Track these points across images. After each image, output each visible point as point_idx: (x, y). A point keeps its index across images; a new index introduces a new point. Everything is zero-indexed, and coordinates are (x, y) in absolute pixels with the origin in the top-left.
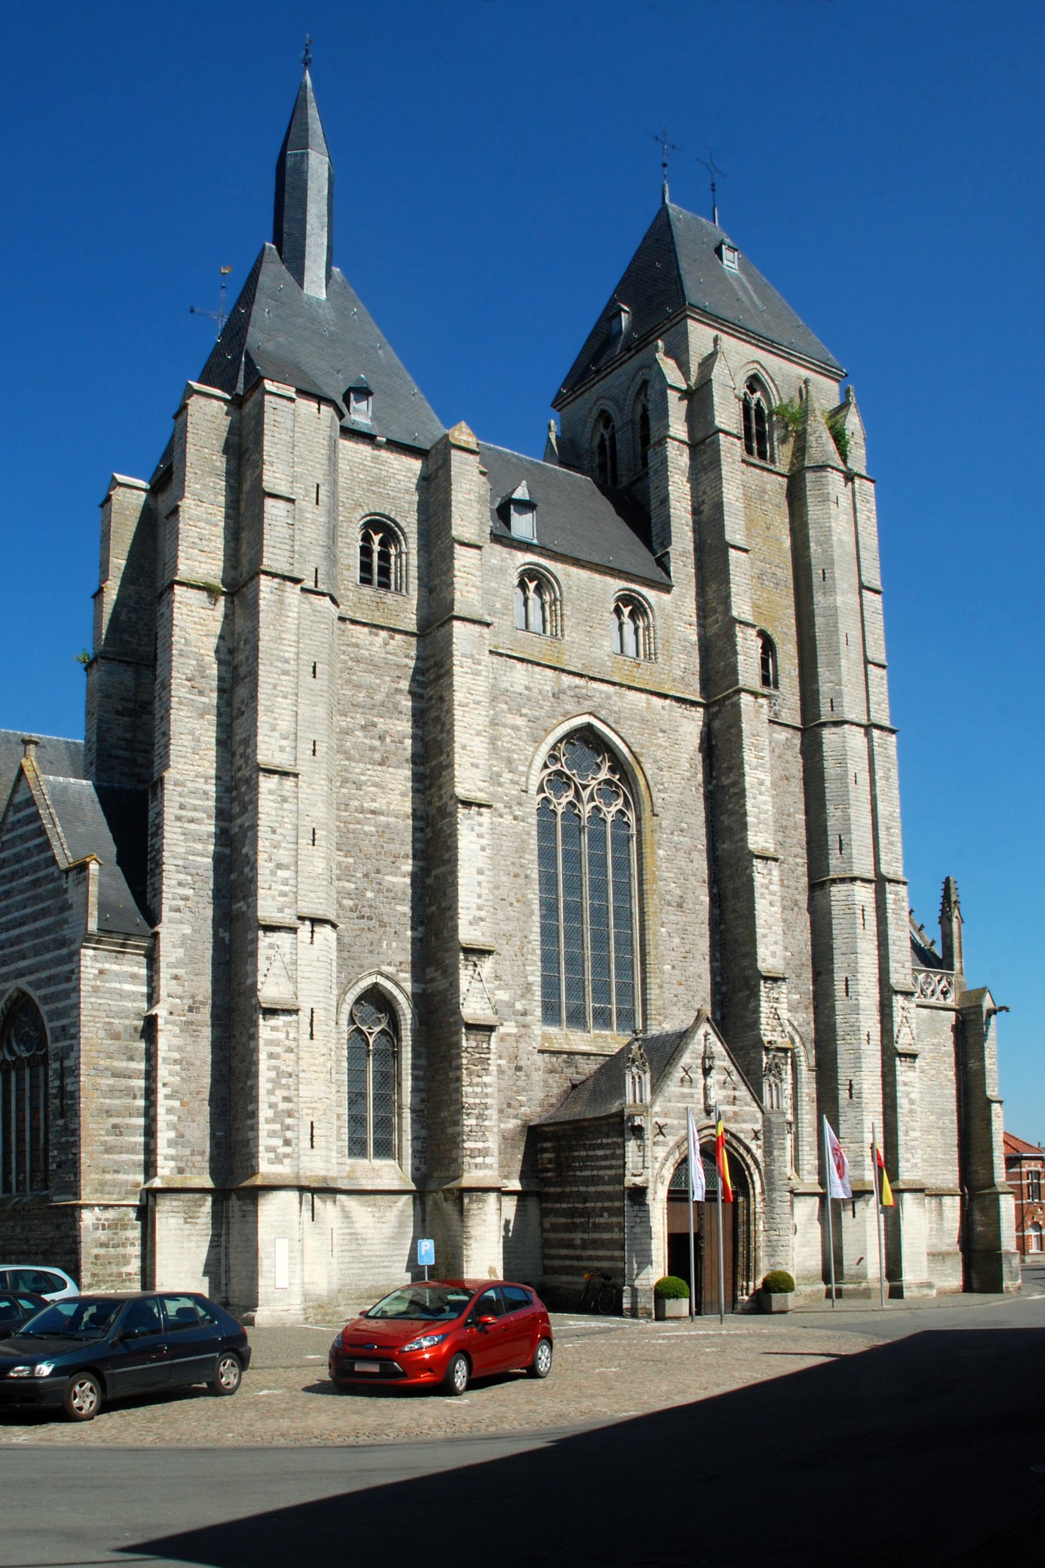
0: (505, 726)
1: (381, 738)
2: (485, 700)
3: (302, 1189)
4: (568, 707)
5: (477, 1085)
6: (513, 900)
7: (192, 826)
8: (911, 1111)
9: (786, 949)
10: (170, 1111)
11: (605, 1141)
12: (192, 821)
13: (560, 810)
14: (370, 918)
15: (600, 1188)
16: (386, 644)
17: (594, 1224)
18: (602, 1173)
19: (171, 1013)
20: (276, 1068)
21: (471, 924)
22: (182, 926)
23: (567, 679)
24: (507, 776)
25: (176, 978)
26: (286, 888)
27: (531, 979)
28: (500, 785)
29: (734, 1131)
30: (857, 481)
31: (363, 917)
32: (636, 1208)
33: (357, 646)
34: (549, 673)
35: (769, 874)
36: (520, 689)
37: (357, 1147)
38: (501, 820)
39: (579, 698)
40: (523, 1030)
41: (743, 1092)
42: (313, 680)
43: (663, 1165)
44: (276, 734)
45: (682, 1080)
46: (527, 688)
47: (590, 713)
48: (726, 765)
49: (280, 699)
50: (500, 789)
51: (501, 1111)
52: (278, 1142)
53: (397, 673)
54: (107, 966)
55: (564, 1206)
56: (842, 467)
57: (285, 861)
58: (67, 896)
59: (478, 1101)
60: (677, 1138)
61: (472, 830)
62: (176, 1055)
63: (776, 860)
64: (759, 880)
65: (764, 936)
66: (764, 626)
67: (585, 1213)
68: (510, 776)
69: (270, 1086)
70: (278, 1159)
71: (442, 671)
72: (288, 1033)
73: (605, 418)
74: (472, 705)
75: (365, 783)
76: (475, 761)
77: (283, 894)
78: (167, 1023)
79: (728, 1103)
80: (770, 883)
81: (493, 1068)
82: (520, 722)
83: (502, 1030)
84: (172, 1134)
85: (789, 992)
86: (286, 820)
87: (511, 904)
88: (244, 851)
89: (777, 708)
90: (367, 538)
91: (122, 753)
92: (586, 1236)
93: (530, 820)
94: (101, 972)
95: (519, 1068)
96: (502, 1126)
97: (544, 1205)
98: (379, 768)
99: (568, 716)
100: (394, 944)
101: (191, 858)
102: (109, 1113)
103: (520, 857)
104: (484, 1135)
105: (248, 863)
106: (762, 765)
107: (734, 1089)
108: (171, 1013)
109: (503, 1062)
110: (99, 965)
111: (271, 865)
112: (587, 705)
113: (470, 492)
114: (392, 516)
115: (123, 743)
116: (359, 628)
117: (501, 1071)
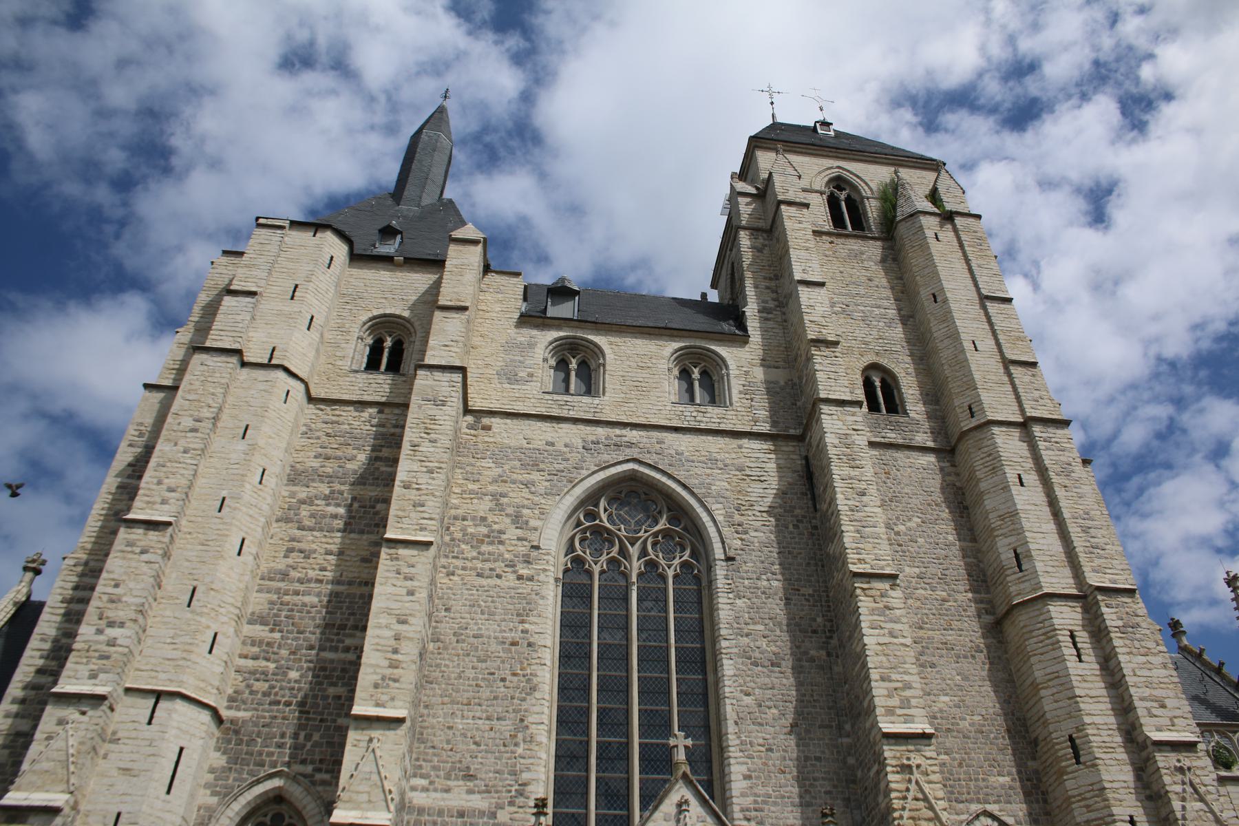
6: (507, 674)
28: (501, 543)
30: (959, 221)
31: (278, 703)
38: (498, 582)
56: (936, 210)
87: (503, 680)
103: (522, 622)
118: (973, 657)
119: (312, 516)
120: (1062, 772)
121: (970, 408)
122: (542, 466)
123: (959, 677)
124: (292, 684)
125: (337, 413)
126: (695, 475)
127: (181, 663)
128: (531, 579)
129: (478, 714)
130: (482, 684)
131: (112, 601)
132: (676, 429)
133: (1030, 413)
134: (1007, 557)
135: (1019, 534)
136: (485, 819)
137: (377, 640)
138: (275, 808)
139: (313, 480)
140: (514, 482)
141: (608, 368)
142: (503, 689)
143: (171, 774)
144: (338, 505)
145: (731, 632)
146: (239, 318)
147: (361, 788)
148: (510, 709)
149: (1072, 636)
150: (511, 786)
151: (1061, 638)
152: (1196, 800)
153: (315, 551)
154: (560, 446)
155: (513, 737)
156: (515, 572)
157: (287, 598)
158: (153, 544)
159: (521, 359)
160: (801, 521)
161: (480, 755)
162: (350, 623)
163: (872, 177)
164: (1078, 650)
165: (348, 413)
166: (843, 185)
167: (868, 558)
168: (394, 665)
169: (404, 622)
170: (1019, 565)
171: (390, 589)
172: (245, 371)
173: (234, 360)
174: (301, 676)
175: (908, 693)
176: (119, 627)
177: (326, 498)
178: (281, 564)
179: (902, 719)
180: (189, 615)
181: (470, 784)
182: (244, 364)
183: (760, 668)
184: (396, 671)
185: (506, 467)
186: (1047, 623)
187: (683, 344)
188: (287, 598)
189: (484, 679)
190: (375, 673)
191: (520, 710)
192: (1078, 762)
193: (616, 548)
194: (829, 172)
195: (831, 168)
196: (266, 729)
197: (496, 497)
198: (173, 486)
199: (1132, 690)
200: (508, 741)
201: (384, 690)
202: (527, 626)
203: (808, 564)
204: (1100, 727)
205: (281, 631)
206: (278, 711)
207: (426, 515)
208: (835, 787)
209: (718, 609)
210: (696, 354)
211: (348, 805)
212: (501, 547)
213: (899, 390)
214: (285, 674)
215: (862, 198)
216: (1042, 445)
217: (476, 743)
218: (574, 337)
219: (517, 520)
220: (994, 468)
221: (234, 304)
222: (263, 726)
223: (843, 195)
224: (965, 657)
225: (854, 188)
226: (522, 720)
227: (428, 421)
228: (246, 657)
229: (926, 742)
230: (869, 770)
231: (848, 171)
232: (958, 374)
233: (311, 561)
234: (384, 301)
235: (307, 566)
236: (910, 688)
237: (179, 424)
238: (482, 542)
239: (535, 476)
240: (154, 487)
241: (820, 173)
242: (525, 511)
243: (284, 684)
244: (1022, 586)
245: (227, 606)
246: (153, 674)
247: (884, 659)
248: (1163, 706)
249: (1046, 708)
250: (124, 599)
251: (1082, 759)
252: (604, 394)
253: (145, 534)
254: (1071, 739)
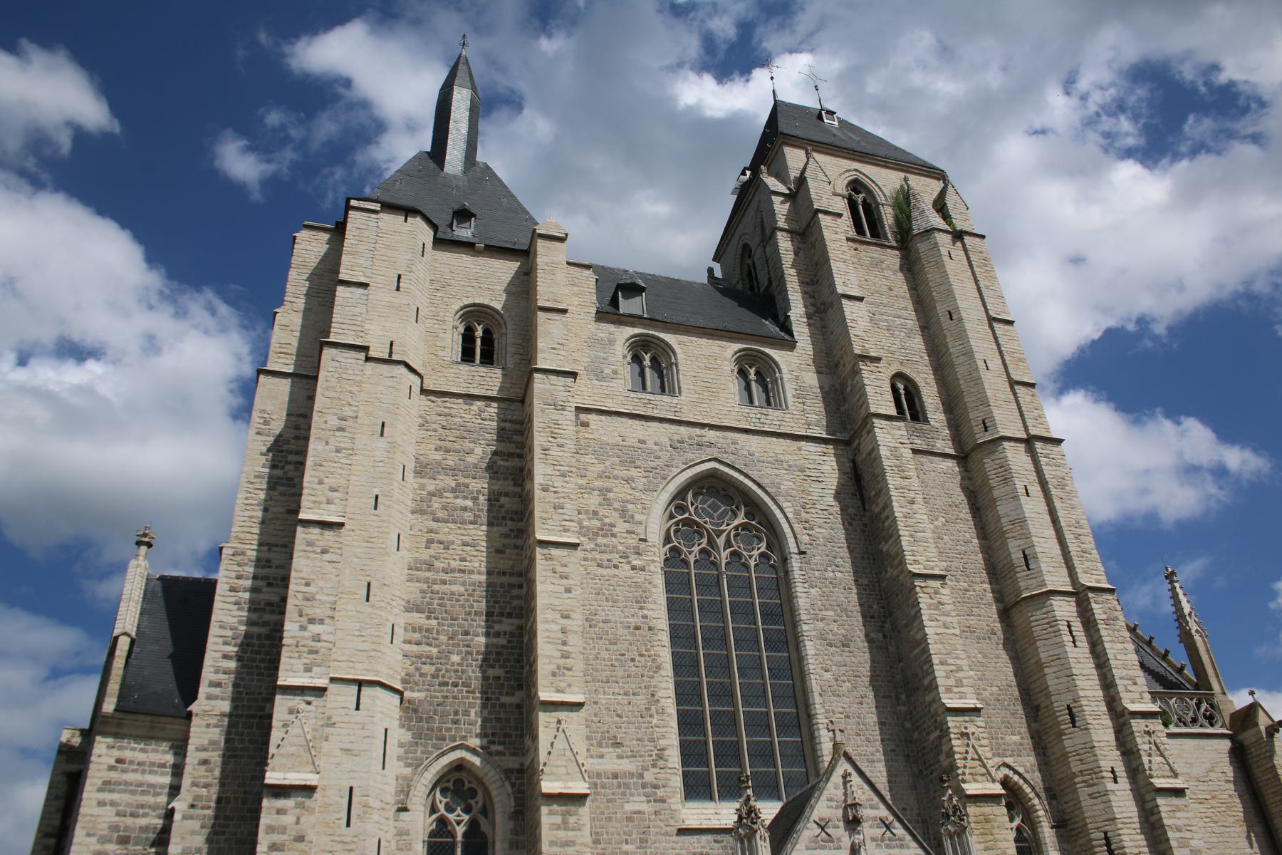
6: (635, 654)
13: (692, 559)
16: (482, 411)
28: (613, 535)
30: (967, 239)
31: (446, 684)
38: (616, 572)
47: (715, 460)
48: (873, 493)
56: (949, 229)
87: (633, 660)
98: (471, 526)
103: (641, 608)
108: (192, 806)
118: (989, 638)
119: (444, 508)
120: (1061, 733)
121: (984, 423)
122: (638, 463)
123: (980, 656)
124: (456, 667)
125: (448, 405)
126: (766, 474)
127: (372, 654)
128: (643, 569)
129: (617, 691)
130: (617, 665)
131: (308, 600)
132: (746, 431)
133: (1033, 431)
134: (1017, 557)
135: (1027, 538)
136: (635, 780)
137: (547, 634)
138: (457, 775)
139: (438, 473)
140: (616, 478)
141: (680, 367)
142: (633, 668)
143: (382, 752)
144: (465, 498)
145: (809, 617)
146: (357, 311)
147: (559, 763)
148: (642, 685)
149: (1069, 626)
150: (652, 751)
151: (1061, 627)
152: (1158, 756)
153: (453, 543)
154: (650, 444)
155: (648, 709)
156: (629, 563)
157: (436, 587)
158: (330, 544)
159: (605, 355)
160: (853, 519)
161: (623, 725)
162: (497, 610)
163: (886, 182)
164: (1073, 637)
165: (458, 405)
166: (859, 188)
167: (921, 559)
168: (565, 656)
169: (567, 617)
170: (1027, 565)
171: (552, 588)
172: (370, 365)
173: (362, 355)
174: (462, 659)
175: (960, 675)
176: (319, 624)
177: (453, 490)
178: (425, 555)
179: (957, 696)
180: (370, 610)
181: (619, 750)
182: (368, 359)
183: (834, 648)
184: (567, 661)
185: (608, 463)
186: (1050, 615)
187: (745, 346)
188: (436, 587)
189: (616, 659)
190: (550, 663)
191: (650, 686)
192: (1074, 726)
193: (705, 540)
194: (848, 174)
195: (850, 170)
196: (440, 708)
197: (604, 492)
198: (334, 486)
199: (1115, 671)
200: (644, 713)
201: (561, 678)
202: (645, 612)
203: (863, 557)
204: (1091, 699)
205: (436, 618)
206: (448, 691)
207: (568, 518)
208: (897, 746)
209: (797, 597)
210: (751, 356)
211: (551, 777)
212: (613, 539)
213: (920, 399)
214: (448, 658)
215: (878, 204)
216: (1043, 460)
217: (618, 716)
218: (647, 335)
219: (623, 513)
220: (1005, 479)
221: (349, 295)
222: (438, 705)
223: (860, 198)
224: (984, 639)
225: (869, 192)
226: (653, 695)
227: (553, 426)
228: (410, 642)
229: (977, 714)
230: (928, 734)
231: (864, 175)
232: (972, 390)
233: (451, 552)
234: (470, 289)
235: (449, 557)
236: (962, 670)
237: (326, 422)
238: (597, 534)
239: (633, 473)
240: (317, 486)
241: (840, 175)
242: (630, 506)
243: (448, 667)
244: (1030, 582)
245: (397, 599)
246: (350, 664)
247: (940, 646)
248: (1135, 684)
249: (1049, 683)
250: (318, 597)
251: (1077, 724)
252: (680, 393)
253: (321, 534)
254: (1069, 708)
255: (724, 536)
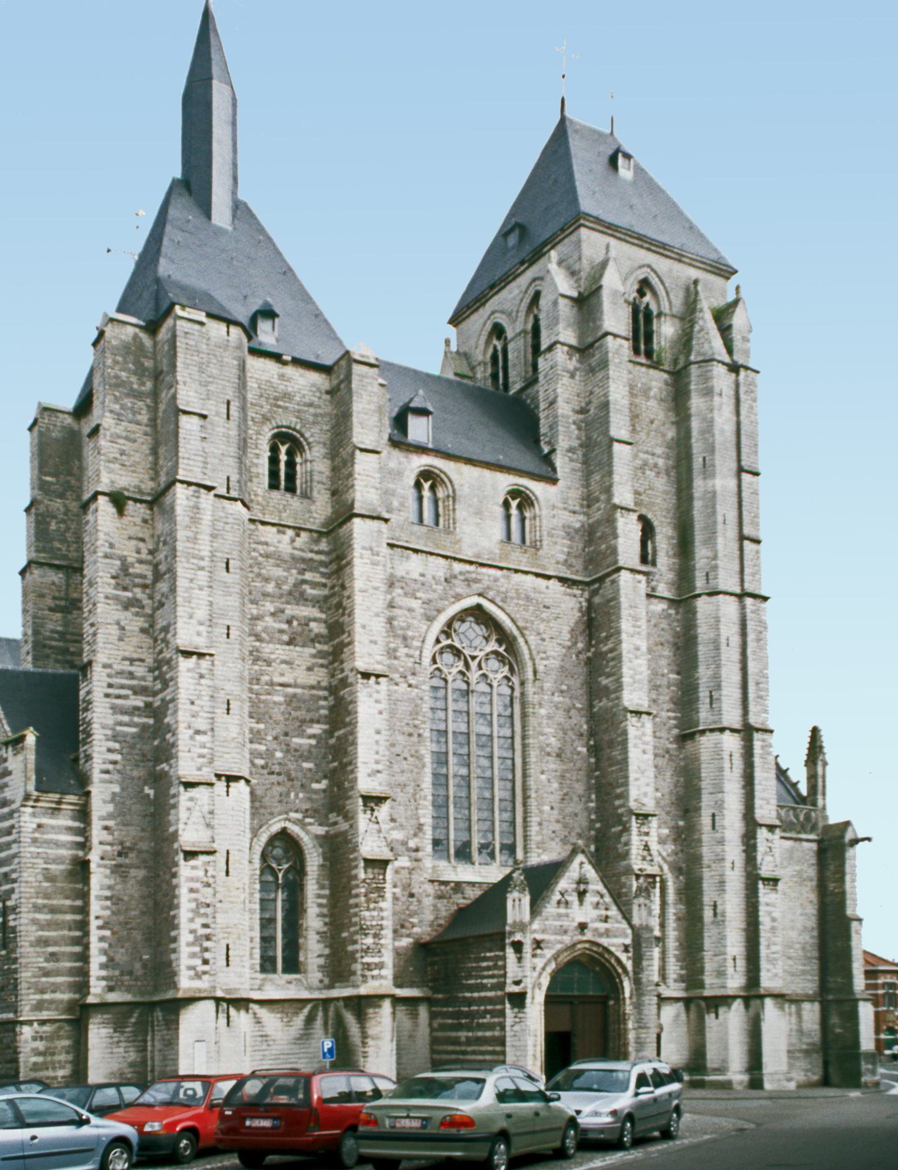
0: (401, 608)
1: (289, 622)
2: (383, 588)
3: (218, 1000)
4: (459, 590)
5: (374, 909)
7: (119, 702)
8: (773, 929)
9: (657, 790)
10: (102, 939)
11: (488, 954)
12: (118, 697)
14: (279, 774)
15: (483, 994)
17: (478, 1023)
18: (485, 981)
19: (102, 858)
20: (196, 900)
21: (369, 775)
22: (112, 786)
23: (458, 567)
24: (402, 651)
25: (106, 828)
26: (205, 751)
27: (422, 821)
28: (396, 658)
29: (606, 945)
32: (516, 1010)
33: (266, 544)
34: (442, 561)
35: (643, 726)
36: (415, 576)
37: (267, 965)
38: (396, 688)
39: (468, 582)
40: (415, 864)
41: (614, 912)
42: (225, 573)
43: (540, 974)
44: (194, 621)
45: (559, 902)
46: (422, 575)
49: (197, 591)
50: (396, 662)
51: (395, 931)
52: (198, 962)
53: (303, 566)
54: (44, 821)
55: (450, 1009)
57: (203, 727)
58: (6, 764)
59: (374, 923)
60: (553, 952)
61: (371, 696)
62: (108, 893)
63: (649, 714)
64: (632, 732)
65: (637, 779)
66: (644, 511)
67: (470, 1015)
68: (406, 650)
69: (190, 915)
70: (198, 976)
71: (344, 562)
72: (206, 871)
73: (498, 331)
74: (371, 591)
75: (274, 660)
76: (374, 638)
77: (202, 756)
78: (99, 866)
79: (601, 921)
80: (644, 734)
81: (388, 895)
82: (415, 604)
83: (397, 864)
84: (104, 959)
85: (659, 827)
86: (203, 693)
88: (166, 720)
89: (654, 583)
90: (274, 450)
91: (54, 643)
92: (470, 1034)
93: (423, 687)
94: (40, 826)
95: (412, 895)
96: (397, 944)
97: (434, 1009)
99: (458, 597)
100: (301, 795)
101: (119, 728)
102: (46, 942)
104: (379, 952)
105: (169, 731)
106: (639, 633)
107: (607, 909)
109: (397, 890)
110: (38, 820)
111: (191, 732)
112: (477, 587)
113: (369, 403)
114: (298, 427)
115: (56, 636)
116: (269, 528)
117: (395, 898)
128: (416, 687)
177: (273, 614)
255: (477, 660)
